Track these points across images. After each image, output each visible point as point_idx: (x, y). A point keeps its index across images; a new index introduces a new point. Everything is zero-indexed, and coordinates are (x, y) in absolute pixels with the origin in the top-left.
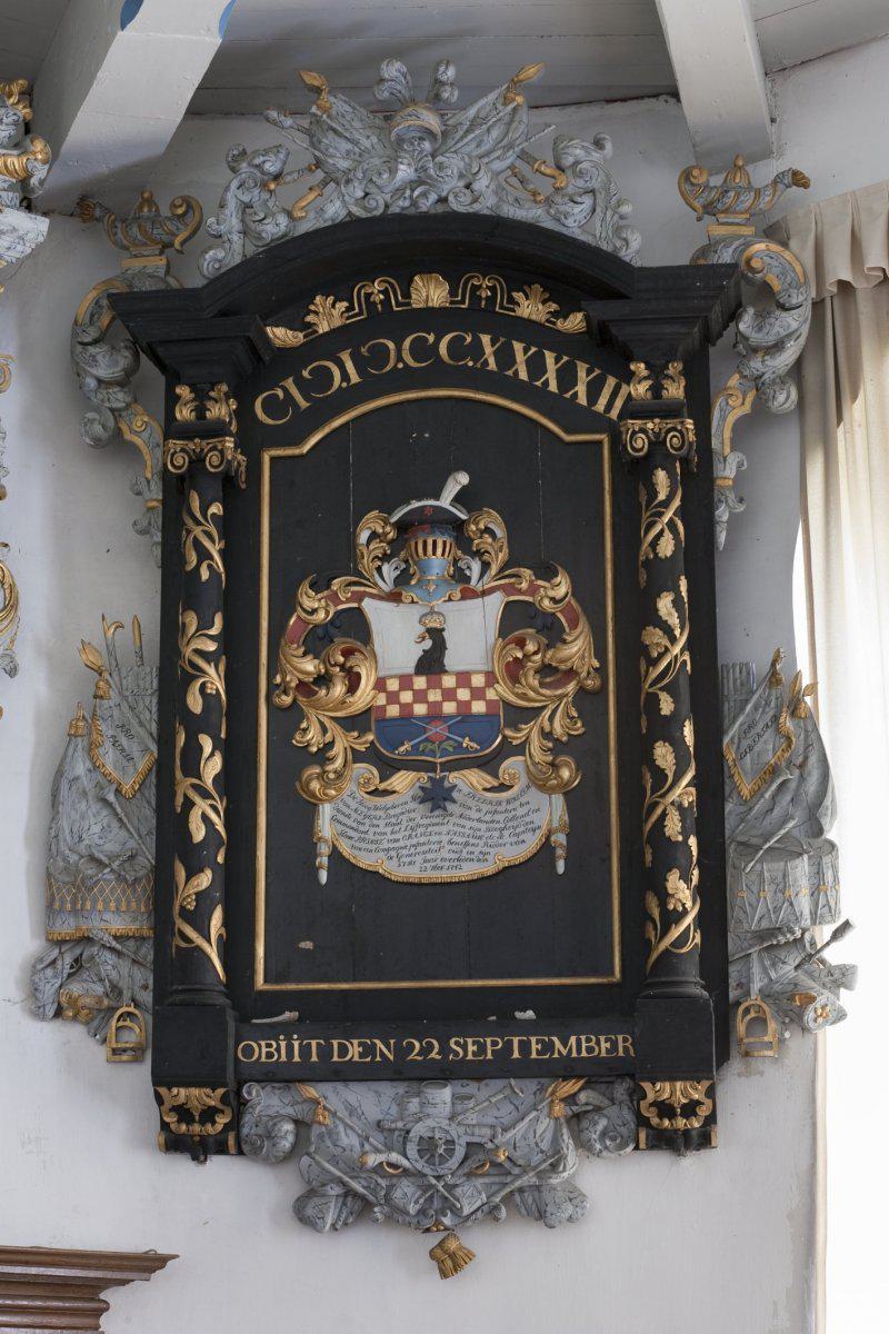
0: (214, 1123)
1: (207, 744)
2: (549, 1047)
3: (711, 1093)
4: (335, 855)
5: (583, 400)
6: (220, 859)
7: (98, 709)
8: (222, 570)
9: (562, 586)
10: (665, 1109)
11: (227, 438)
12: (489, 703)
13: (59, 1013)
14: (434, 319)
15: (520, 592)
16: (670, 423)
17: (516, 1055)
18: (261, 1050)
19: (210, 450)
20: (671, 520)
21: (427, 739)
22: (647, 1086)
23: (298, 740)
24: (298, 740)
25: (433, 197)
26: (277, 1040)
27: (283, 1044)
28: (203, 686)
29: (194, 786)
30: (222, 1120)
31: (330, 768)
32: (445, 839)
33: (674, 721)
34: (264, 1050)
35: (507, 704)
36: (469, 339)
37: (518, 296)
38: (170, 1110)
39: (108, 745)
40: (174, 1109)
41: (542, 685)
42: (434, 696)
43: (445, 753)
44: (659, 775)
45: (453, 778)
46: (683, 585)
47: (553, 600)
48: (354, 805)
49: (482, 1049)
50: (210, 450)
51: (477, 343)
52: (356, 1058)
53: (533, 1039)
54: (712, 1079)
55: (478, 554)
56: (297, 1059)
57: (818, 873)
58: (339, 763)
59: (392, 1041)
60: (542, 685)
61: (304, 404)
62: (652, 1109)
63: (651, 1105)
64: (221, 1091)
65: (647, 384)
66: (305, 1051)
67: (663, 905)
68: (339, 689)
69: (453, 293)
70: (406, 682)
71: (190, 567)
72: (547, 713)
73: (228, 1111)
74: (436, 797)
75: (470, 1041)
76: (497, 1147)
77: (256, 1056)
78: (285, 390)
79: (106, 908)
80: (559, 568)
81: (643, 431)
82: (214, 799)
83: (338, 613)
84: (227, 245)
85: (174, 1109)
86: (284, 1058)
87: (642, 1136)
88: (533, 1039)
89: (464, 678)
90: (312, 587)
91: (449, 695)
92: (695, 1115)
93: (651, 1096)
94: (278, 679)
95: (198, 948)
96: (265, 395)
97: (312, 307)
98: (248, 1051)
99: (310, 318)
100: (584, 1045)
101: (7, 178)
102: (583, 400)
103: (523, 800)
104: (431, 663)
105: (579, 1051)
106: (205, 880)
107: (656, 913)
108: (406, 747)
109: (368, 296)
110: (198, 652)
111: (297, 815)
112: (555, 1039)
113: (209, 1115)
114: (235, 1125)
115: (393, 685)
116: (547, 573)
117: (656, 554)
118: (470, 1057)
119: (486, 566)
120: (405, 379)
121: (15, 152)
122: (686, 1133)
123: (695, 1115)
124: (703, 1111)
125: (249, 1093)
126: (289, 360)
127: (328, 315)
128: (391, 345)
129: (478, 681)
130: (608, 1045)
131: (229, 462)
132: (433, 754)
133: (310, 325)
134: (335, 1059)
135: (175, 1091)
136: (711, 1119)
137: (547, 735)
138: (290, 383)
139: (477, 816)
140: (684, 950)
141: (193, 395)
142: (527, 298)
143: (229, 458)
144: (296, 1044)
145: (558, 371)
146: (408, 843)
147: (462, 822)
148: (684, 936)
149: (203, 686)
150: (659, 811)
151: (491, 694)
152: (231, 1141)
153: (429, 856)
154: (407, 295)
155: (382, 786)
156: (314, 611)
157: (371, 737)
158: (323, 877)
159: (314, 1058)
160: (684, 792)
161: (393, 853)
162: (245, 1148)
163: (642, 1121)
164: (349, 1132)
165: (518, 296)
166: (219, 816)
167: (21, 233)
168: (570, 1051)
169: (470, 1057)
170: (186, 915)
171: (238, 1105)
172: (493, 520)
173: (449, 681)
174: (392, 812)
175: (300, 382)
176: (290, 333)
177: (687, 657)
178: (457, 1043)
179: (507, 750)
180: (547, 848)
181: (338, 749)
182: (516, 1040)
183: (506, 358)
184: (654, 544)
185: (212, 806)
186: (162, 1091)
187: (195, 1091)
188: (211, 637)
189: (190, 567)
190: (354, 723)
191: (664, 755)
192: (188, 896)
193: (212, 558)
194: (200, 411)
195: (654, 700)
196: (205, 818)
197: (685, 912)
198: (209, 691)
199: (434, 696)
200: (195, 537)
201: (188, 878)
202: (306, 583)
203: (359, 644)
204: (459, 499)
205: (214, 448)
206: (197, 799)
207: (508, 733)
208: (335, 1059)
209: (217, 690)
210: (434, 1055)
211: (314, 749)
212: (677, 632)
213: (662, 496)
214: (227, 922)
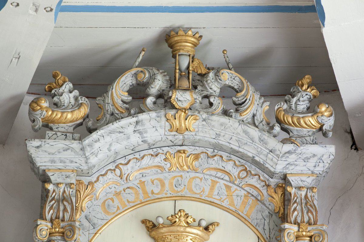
101: (309, 130)
121: (310, 115)
167: (319, 156)
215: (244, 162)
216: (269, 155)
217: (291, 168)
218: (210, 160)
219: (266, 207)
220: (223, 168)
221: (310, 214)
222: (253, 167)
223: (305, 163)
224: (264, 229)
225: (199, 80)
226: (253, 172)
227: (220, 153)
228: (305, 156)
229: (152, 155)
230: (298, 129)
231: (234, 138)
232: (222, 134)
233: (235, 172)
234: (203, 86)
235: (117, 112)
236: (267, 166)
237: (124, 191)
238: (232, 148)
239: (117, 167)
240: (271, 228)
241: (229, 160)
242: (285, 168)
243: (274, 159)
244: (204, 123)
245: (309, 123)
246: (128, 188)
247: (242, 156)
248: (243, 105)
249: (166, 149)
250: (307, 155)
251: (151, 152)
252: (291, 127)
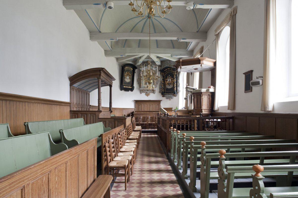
14: (169, 70)
104: (169, 81)
111: (166, 86)
127: (166, 70)
160: (175, 85)
172: (171, 76)
190: (167, 83)
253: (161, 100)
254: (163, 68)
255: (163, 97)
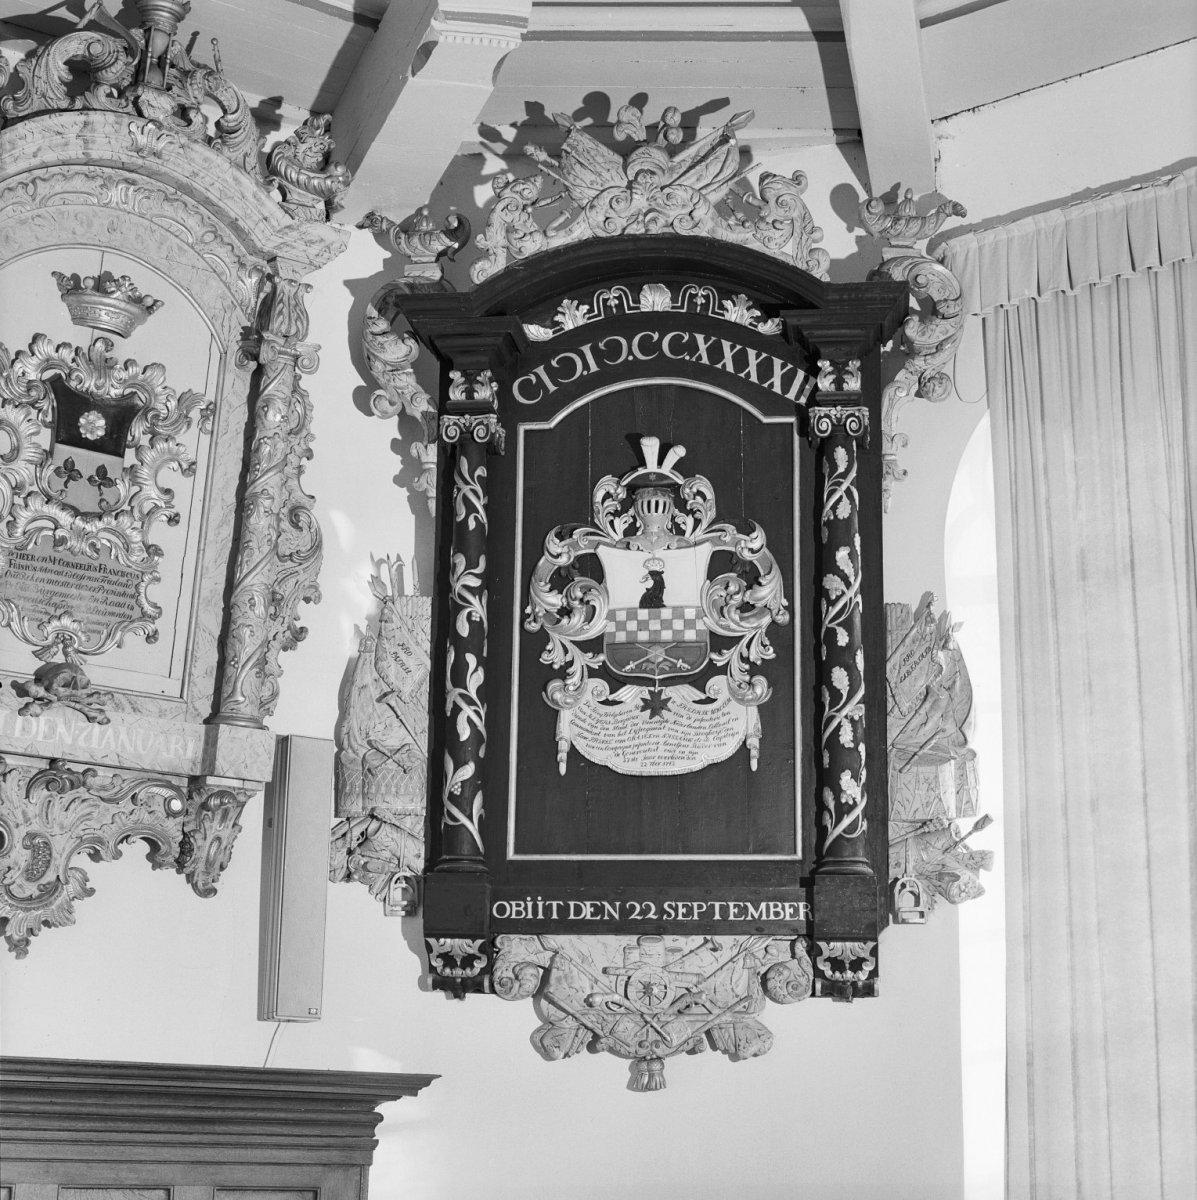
0: (472, 967)
1: (471, 659)
2: (744, 911)
3: (874, 952)
4: (573, 752)
5: (777, 389)
6: (482, 754)
7: (383, 632)
8: (485, 521)
9: (758, 539)
10: (837, 964)
11: (492, 415)
12: (698, 633)
13: (348, 877)
15: (725, 543)
16: (851, 410)
17: (717, 917)
18: (512, 909)
19: (478, 424)
20: (848, 488)
21: (648, 661)
22: (822, 944)
23: (545, 658)
24: (545, 658)
25: (662, 221)
26: (525, 901)
27: (530, 904)
28: (470, 614)
29: (461, 695)
30: (479, 965)
31: (569, 682)
32: (662, 740)
33: (850, 648)
34: (515, 909)
35: (712, 634)
36: (686, 337)
37: (728, 304)
38: (438, 957)
39: (391, 660)
40: (440, 956)
41: (742, 619)
42: (655, 625)
43: (662, 671)
44: (836, 695)
45: (668, 692)
46: (857, 540)
47: (752, 551)
48: (589, 712)
49: (690, 911)
50: (478, 424)
51: (693, 340)
52: (589, 917)
53: (731, 904)
54: (876, 940)
55: (692, 512)
56: (540, 916)
57: (962, 777)
58: (576, 679)
59: (618, 904)
60: (742, 619)
61: (552, 388)
62: (828, 964)
63: (825, 960)
64: (479, 942)
65: (831, 378)
66: (547, 910)
67: (837, 798)
68: (577, 619)
69: (674, 299)
70: (632, 614)
71: (460, 518)
72: (745, 641)
73: (485, 958)
74: (655, 706)
75: (680, 904)
76: (701, 992)
77: (508, 913)
78: (536, 375)
79: (388, 792)
80: (757, 525)
81: (827, 416)
82: (476, 704)
83: (579, 558)
84: (492, 258)
85: (440, 956)
86: (530, 916)
87: (818, 986)
88: (731, 904)
89: (678, 612)
90: (557, 536)
91: (667, 624)
92: (861, 969)
93: (826, 954)
94: (528, 610)
95: (463, 826)
96: (520, 380)
97: (560, 309)
98: (502, 910)
99: (558, 318)
100: (772, 910)
102: (777, 389)
103: (725, 710)
104: (653, 599)
105: (768, 916)
106: (468, 771)
107: (832, 805)
108: (632, 665)
109: (605, 301)
110: (465, 587)
111: (542, 721)
112: (749, 904)
113: (468, 961)
114: (489, 970)
115: (622, 616)
116: (747, 530)
117: (836, 516)
118: (680, 917)
119: (697, 522)
120: (633, 369)
121: (322, 176)
122: (854, 984)
123: (861, 969)
124: (868, 968)
125: (502, 943)
126: (544, 351)
127: (573, 316)
128: (623, 341)
129: (690, 614)
130: (792, 910)
131: (493, 435)
132: (652, 672)
133: (558, 323)
134: (572, 917)
135: (442, 940)
136: (874, 973)
137: (745, 659)
138: (540, 370)
139: (687, 722)
140: (854, 836)
141: (463, 379)
142: (735, 305)
143: (493, 431)
144: (540, 904)
145: (759, 365)
146: (632, 743)
147: (676, 727)
148: (853, 827)
149: (470, 614)
150: (834, 724)
151: (700, 626)
152: (486, 983)
153: (648, 754)
154: (637, 301)
155: (611, 698)
156: (559, 556)
157: (602, 657)
158: (563, 769)
159: (555, 916)
160: (855, 709)
161: (620, 751)
162: (497, 987)
163: (818, 973)
164: (582, 975)
165: (728, 304)
166: (480, 718)
168: (761, 915)
169: (680, 917)
170: (452, 796)
171: (489, 950)
172: (703, 484)
173: (666, 613)
174: (619, 718)
175: (549, 370)
176: (542, 330)
177: (859, 599)
178: (670, 906)
179: (713, 670)
180: (744, 749)
181: (576, 668)
182: (717, 905)
183: (716, 353)
184: (834, 508)
185: (477, 713)
186: (432, 941)
187: (458, 941)
188: (476, 575)
189: (460, 518)
190: (592, 646)
191: (840, 678)
192: (456, 784)
193: (478, 512)
194: (470, 392)
195: (832, 633)
196: (470, 721)
197: (855, 804)
198: (474, 619)
199: (655, 625)
200: (464, 494)
201: (456, 769)
202: (553, 532)
203: (593, 583)
204: (678, 467)
205: (481, 423)
206: (463, 704)
207: (714, 656)
208: (572, 917)
209: (481, 618)
210: (651, 915)
211: (556, 667)
212: (852, 579)
213: (841, 469)
214: (484, 806)
215: (216, 220)
216: (261, 224)
217: (285, 249)
218: (166, 205)
219: (232, 294)
220: (182, 222)
221: (299, 323)
222: (228, 232)
223: (305, 247)
224: (223, 326)
225: (176, 77)
226: (226, 240)
227: (185, 198)
228: (308, 238)
229: (86, 175)
230: (302, 192)
231: (217, 185)
232: (202, 174)
233: (199, 230)
234: (183, 88)
235: (52, 96)
236: (253, 237)
237: (33, 219)
238: (208, 198)
239: (33, 182)
240: (233, 327)
241: (197, 213)
242: (278, 247)
243: (266, 232)
244: (181, 151)
245: (289, 174)
246: (39, 216)
247: (218, 212)
248: (233, 135)
249: (108, 171)
250: (312, 238)
251: (85, 168)
252: (291, 186)
253: (411, 1084)
254: (532, 246)
255: (457, 989)
